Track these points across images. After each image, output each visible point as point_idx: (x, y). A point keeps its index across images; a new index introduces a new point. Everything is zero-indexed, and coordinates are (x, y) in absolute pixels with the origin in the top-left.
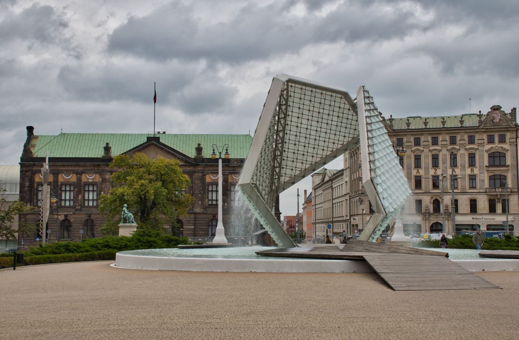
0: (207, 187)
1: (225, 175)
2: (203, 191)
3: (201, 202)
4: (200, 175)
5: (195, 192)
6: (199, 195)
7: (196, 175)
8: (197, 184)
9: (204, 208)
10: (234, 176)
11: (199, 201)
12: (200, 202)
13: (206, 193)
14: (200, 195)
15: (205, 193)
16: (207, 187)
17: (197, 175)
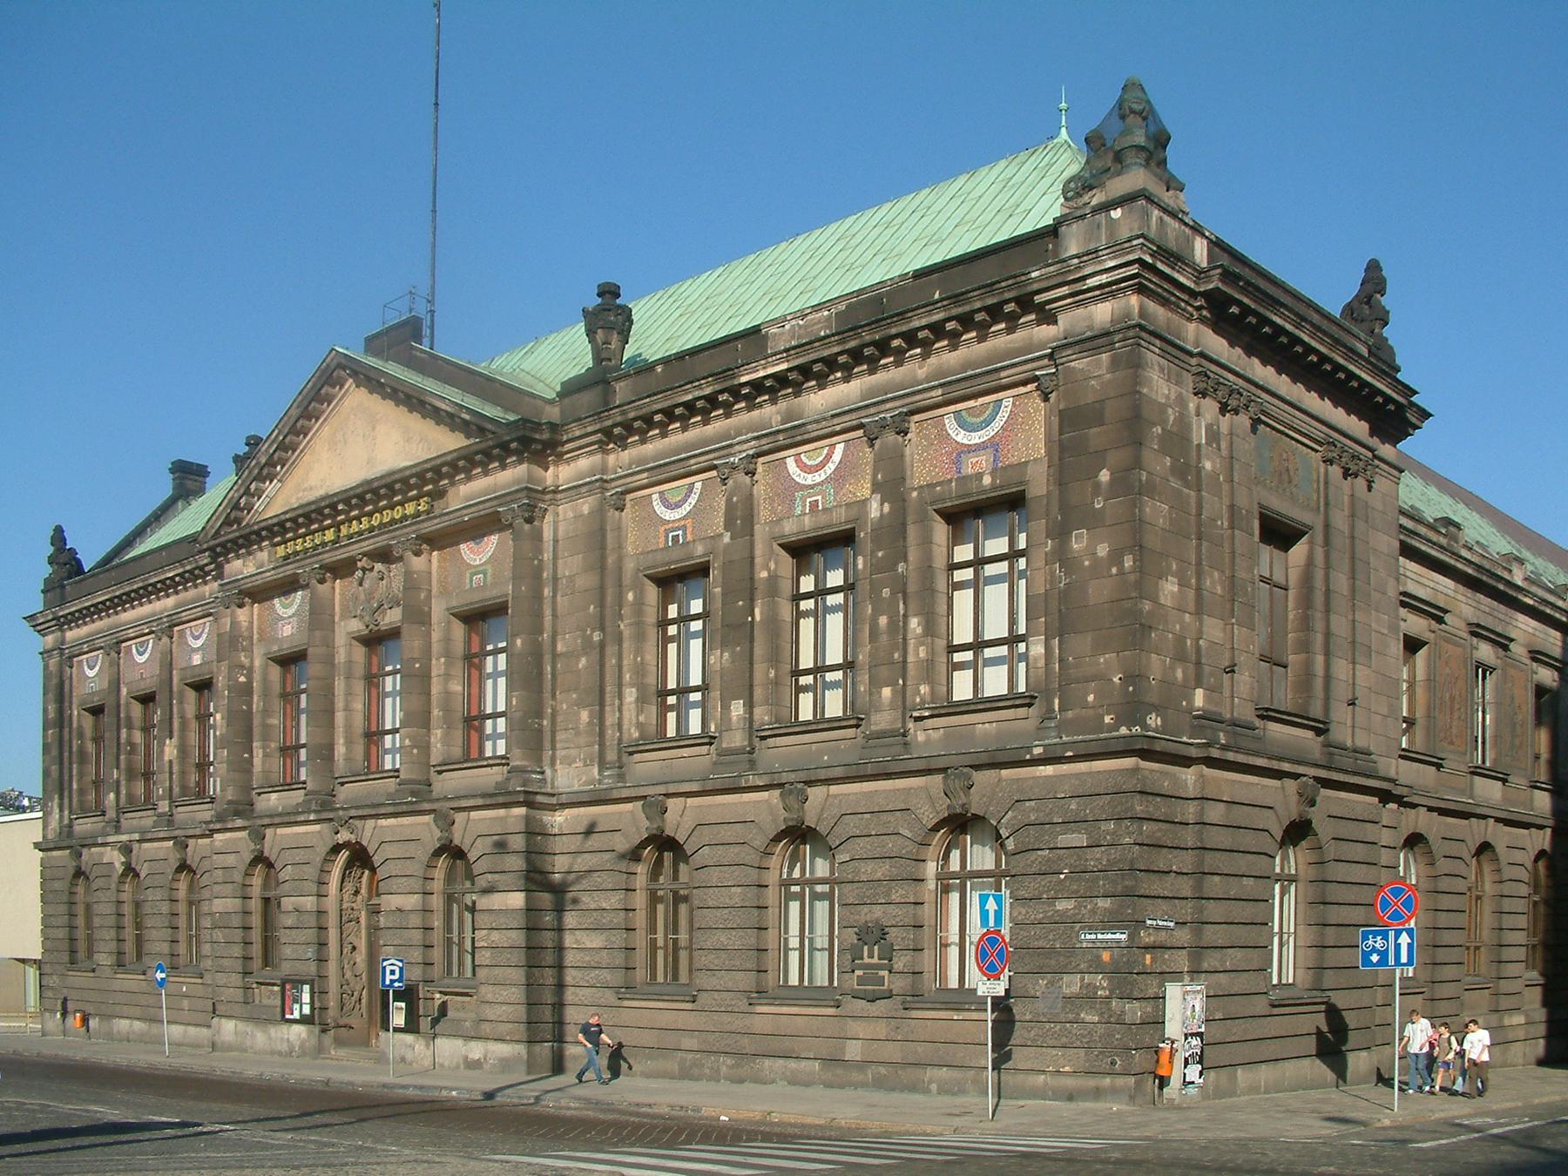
0: (630, 596)
1: (734, 467)
2: (602, 629)
3: (590, 716)
4: (586, 509)
5: (560, 647)
6: (578, 658)
7: (565, 511)
8: (571, 578)
9: (611, 756)
10: (799, 462)
11: (581, 704)
12: (585, 715)
13: (626, 645)
14: (583, 661)
15: (619, 640)
16: (630, 596)
17: (571, 514)
